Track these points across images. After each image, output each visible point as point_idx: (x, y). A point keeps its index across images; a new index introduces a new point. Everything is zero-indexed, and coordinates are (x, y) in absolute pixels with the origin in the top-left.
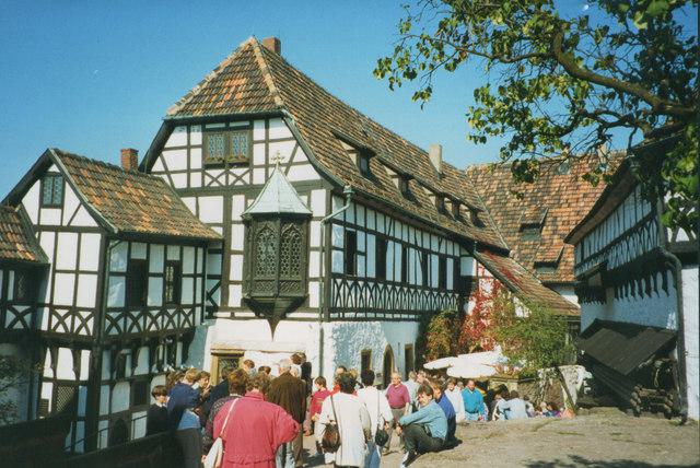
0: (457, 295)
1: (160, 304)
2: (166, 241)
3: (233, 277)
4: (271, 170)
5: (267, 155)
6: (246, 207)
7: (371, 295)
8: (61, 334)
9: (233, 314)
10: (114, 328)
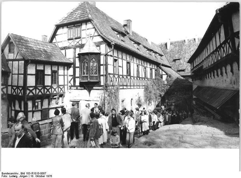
1: (50, 85)
2: (52, 64)
3: (76, 76)
6: (80, 51)
8: (48, 94)
9: (77, 88)
10: (40, 92)
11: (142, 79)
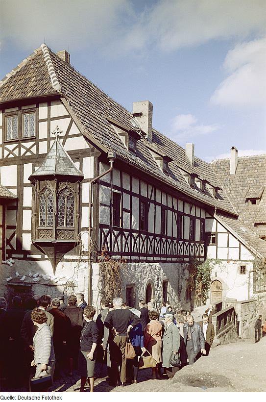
0: (202, 245)
4: (52, 142)
5: (49, 130)
6: (33, 171)
7: (135, 243)
11: (172, 241)
